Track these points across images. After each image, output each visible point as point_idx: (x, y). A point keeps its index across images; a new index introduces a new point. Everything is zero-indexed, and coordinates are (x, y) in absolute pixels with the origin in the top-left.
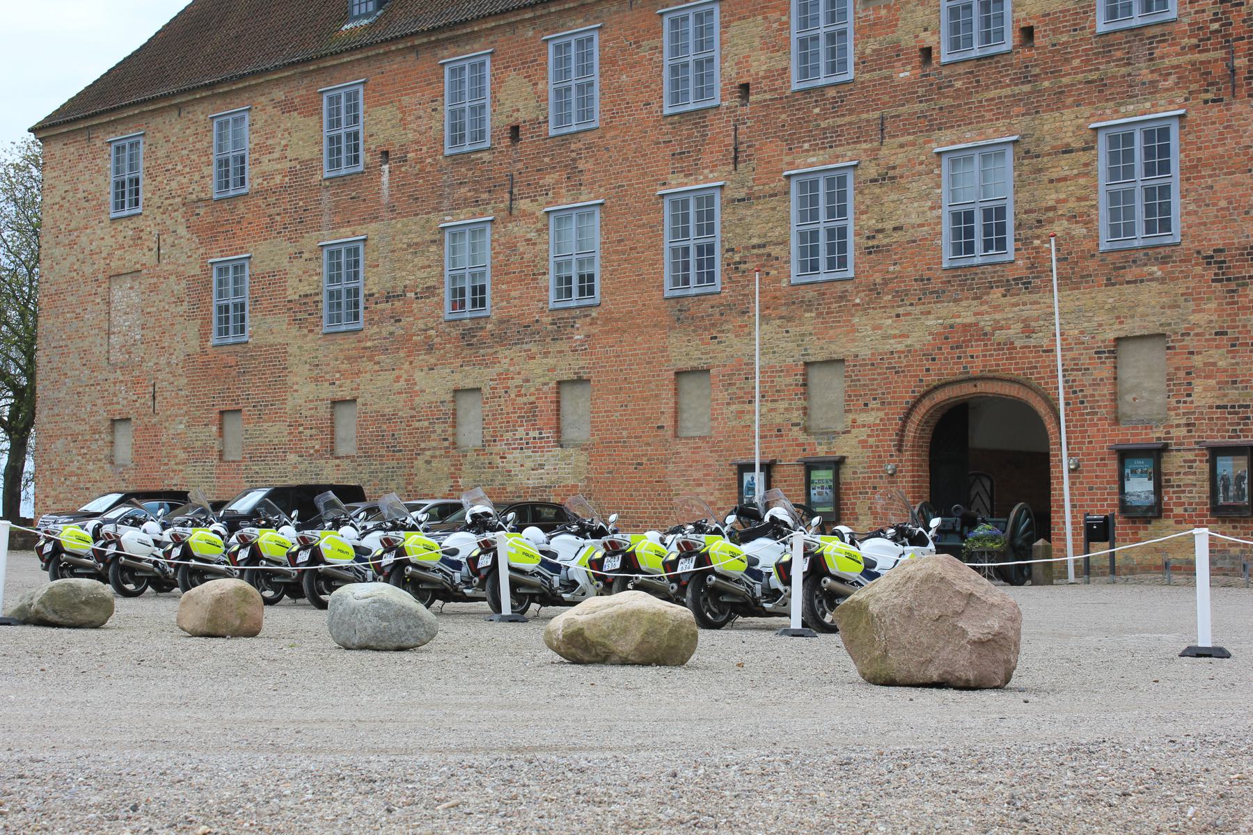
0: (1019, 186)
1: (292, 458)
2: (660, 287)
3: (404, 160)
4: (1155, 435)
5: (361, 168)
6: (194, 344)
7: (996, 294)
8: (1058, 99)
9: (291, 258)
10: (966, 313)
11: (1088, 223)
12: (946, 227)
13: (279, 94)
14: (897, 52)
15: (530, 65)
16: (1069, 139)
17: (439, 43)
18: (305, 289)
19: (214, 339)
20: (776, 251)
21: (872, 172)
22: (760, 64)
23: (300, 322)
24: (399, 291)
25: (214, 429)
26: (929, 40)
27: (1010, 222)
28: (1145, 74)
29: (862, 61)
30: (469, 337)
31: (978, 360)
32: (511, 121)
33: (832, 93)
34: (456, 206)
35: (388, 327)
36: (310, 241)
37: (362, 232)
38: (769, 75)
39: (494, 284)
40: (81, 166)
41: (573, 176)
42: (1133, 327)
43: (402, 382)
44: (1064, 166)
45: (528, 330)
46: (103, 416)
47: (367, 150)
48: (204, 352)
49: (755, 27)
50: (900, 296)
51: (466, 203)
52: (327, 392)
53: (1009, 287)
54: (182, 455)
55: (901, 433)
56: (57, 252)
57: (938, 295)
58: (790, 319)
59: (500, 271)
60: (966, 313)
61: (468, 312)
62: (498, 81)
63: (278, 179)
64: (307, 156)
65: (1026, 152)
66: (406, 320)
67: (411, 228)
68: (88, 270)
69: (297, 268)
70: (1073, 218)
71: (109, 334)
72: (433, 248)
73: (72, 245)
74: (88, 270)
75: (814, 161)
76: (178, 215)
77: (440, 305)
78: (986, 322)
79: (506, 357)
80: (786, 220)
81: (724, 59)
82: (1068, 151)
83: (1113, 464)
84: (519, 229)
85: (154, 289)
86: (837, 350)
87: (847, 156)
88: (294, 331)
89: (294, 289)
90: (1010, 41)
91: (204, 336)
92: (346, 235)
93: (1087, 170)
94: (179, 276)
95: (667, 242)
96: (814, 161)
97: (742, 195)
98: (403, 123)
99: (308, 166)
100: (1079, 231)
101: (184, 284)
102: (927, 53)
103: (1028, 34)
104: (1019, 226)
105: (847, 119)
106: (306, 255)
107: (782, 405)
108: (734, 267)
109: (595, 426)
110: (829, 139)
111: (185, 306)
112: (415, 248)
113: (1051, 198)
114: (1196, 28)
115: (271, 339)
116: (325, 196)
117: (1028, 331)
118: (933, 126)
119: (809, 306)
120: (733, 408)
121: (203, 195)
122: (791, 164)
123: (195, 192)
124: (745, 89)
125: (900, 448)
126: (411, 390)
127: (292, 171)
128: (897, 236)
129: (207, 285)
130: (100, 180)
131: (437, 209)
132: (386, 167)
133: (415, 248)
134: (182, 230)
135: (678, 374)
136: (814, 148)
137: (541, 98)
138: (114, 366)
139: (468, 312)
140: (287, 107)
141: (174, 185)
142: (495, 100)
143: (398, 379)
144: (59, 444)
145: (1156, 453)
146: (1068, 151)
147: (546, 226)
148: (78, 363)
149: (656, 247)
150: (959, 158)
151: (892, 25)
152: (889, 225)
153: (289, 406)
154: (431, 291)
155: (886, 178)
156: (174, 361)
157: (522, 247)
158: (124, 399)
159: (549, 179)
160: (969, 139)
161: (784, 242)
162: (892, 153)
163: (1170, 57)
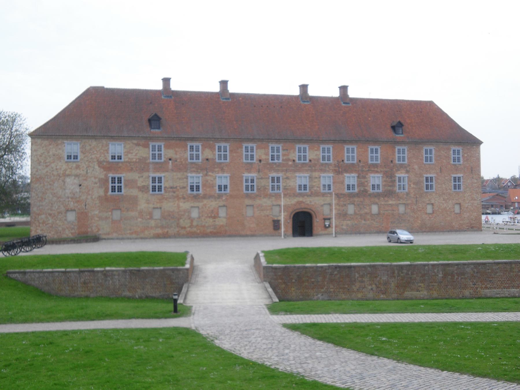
0: (309, 182)
1: (139, 220)
2: (243, 191)
3: (176, 161)
4: (329, 217)
5: (163, 160)
6: (101, 192)
7: (306, 197)
8: (315, 171)
9: (139, 177)
10: (301, 199)
11: (319, 187)
12: (298, 187)
13: (135, 142)
14: (289, 160)
15: (212, 148)
16: (317, 176)
17: (188, 140)
18: (144, 184)
19: (110, 192)
20: (267, 187)
21: (285, 177)
22: (263, 157)
23: (142, 191)
24: (175, 186)
25: (110, 213)
26: (294, 159)
27: (308, 187)
28: (328, 169)
29: (283, 160)
30: (196, 198)
31: (303, 206)
32: (207, 158)
33: (278, 164)
34: (191, 172)
35: (171, 194)
36: (145, 174)
37: (162, 175)
38: (265, 159)
39: (203, 188)
40: (51, 146)
41: (223, 170)
42: (326, 202)
43: (176, 205)
44: (316, 180)
45: (211, 197)
46: (63, 209)
47: (165, 157)
48: (106, 195)
49: (263, 151)
50: (290, 196)
51: (194, 171)
52: (151, 206)
53: (308, 196)
54: (97, 219)
55: (290, 216)
56: (40, 167)
57: (296, 196)
58: (270, 198)
59: (204, 185)
60: (301, 199)
61: (195, 192)
62: (203, 150)
63: (134, 160)
64: (144, 156)
65: (310, 177)
66: (177, 193)
67: (179, 175)
68: (55, 173)
69: (141, 179)
70: (317, 187)
71: (65, 189)
72: (185, 179)
73: (47, 166)
74: (55, 173)
75: (275, 175)
76: (96, 164)
77: (187, 190)
78: (304, 201)
79: (205, 201)
80: (269, 182)
81: (256, 155)
82: (316, 178)
83: (323, 221)
84: (208, 178)
85: (85, 180)
86: (279, 203)
87: (280, 175)
88: (140, 193)
89: (140, 183)
90: (308, 161)
91: (106, 191)
92: (157, 175)
93: (319, 181)
94: (95, 178)
95: (244, 184)
96: (275, 175)
97: (260, 177)
98: (176, 154)
99: (146, 159)
100: (318, 189)
101: (97, 180)
102: (294, 161)
103: (310, 161)
104: (309, 187)
105: (280, 168)
106: (144, 177)
107: (268, 212)
108: (258, 189)
109: (227, 214)
110: (277, 171)
111: (98, 184)
112: (180, 179)
113: (314, 184)
114: (335, 164)
115: (132, 194)
116: (151, 166)
117: (311, 202)
118: (295, 171)
119: (273, 196)
120: (259, 212)
121: (106, 160)
122: (270, 174)
123: (102, 159)
124: (260, 161)
125: (290, 218)
126: (179, 207)
127: (139, 159)
128: (290, 187)
129: (107, 181)
130: (61, 151)
131: (186, 172)
132: (170, 162)
133: (180, 179)
134: (97, 167)
135: (247, 206)
136: (274, 172)
137: (214, 155)
138: (68, 198)
139: (195, 192)
140: (138, 145)
141: (93, 156)
142: (202, 153)
143: (174, 204)
144: (43, 216)
145: (329, 219)
146: (316, 178)
147: (216, 178)
148: (51, 196)
149: (242, 184)
150: (300, 177)
151: (288, 155)
152: (288, 185)
153: (139, 208)
154: (184, 188)
155: (287, 178)
156: (94, 197)
157: (209, 181)
158: (72, 205)
159: (216, 170)
160: (301, 175)
161: (269, 186)
162: (289, 174)
163: (331, 168)
